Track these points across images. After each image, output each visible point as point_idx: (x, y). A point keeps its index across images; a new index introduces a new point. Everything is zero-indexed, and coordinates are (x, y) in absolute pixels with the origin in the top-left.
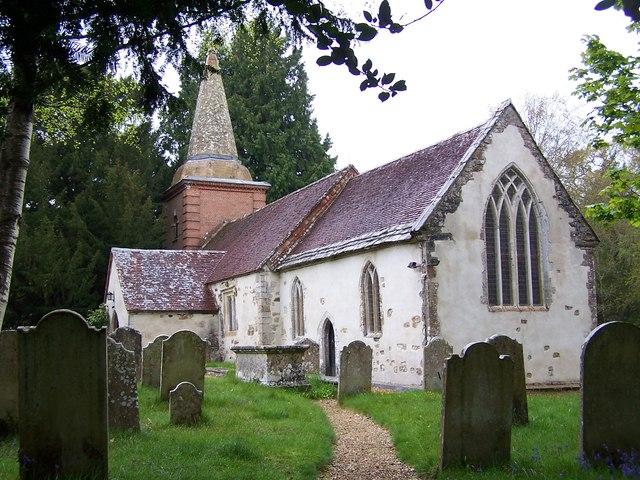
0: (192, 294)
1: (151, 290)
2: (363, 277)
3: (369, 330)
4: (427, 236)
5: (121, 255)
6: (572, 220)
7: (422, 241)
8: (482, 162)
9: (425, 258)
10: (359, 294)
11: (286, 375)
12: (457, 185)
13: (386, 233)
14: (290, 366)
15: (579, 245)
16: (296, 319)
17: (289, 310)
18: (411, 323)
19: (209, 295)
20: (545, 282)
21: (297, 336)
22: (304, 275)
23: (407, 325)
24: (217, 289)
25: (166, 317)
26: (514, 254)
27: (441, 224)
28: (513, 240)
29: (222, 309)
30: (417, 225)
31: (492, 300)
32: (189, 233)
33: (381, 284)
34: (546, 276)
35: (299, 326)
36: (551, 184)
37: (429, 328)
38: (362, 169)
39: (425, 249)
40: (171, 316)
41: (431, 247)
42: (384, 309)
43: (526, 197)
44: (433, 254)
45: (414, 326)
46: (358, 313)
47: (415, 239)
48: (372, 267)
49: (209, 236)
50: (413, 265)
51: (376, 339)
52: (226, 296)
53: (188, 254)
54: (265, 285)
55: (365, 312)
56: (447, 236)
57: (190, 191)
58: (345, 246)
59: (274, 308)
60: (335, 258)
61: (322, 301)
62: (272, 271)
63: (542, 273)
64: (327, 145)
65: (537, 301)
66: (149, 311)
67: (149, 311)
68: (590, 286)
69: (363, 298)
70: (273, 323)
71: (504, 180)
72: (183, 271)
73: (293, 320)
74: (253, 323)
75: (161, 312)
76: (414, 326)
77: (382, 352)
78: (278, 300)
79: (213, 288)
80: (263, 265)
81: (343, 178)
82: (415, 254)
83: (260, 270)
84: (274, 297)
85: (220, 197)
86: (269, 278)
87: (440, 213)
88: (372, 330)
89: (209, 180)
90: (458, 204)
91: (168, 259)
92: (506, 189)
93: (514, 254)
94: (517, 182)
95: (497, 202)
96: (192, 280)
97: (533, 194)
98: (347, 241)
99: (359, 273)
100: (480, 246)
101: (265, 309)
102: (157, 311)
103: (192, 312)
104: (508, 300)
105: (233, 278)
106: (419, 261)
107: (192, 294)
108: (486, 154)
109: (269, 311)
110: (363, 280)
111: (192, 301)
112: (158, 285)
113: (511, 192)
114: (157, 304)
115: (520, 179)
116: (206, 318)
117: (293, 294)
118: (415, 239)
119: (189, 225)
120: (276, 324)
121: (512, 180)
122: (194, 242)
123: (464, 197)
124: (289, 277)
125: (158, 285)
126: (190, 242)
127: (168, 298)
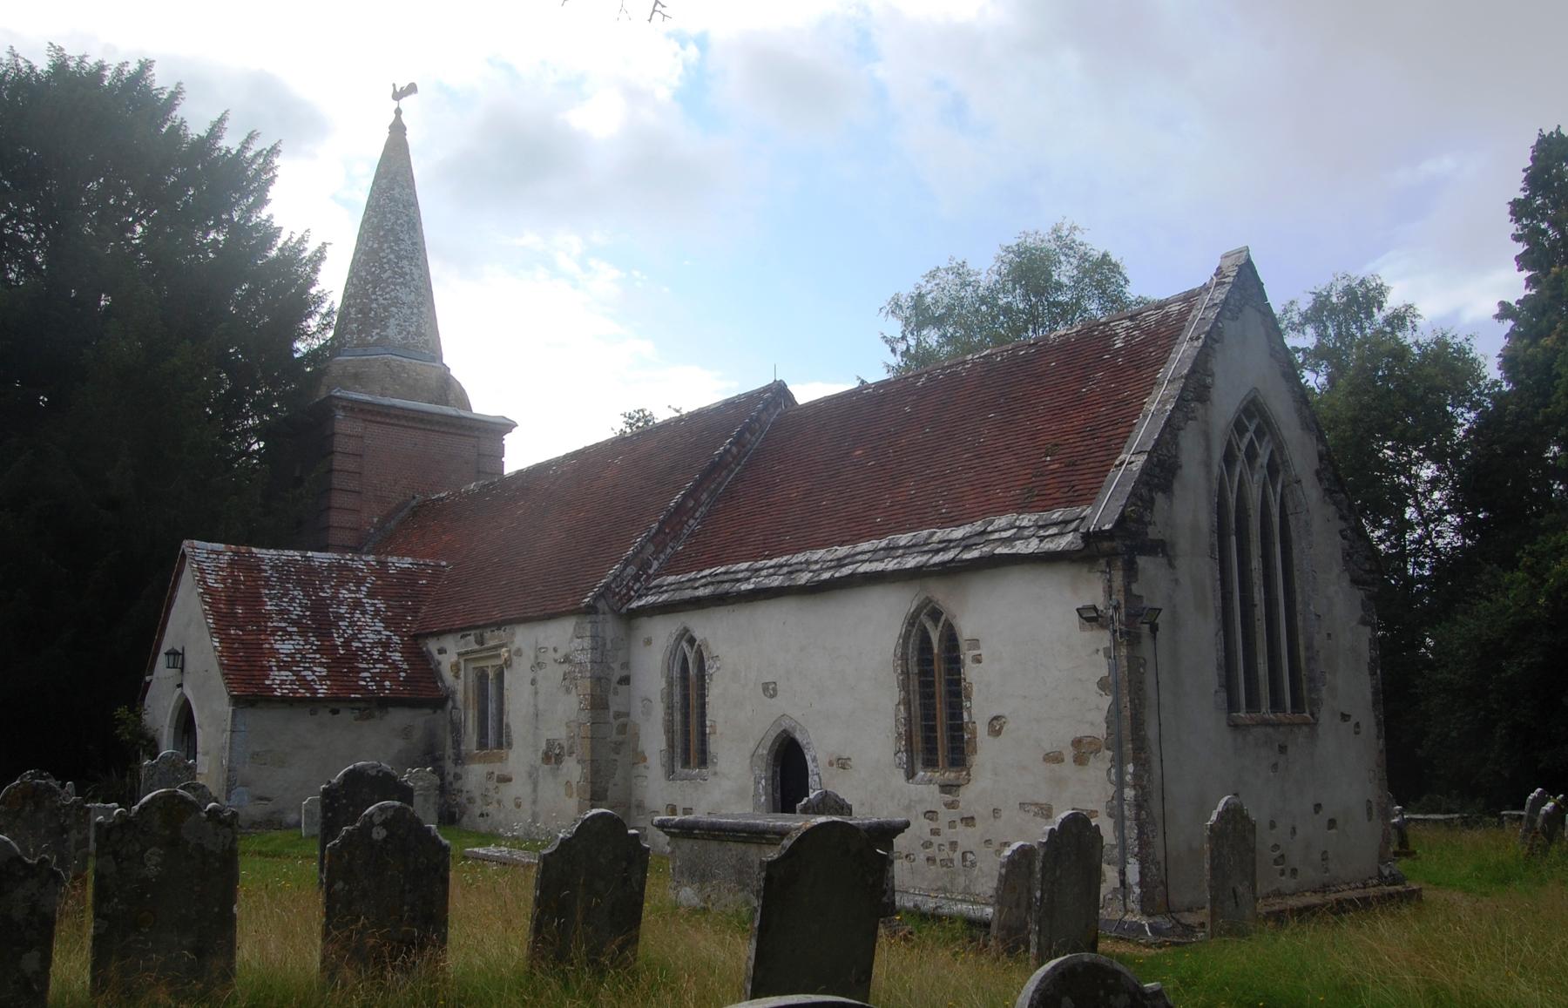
0: (384, 659)
2: (906, 638)
3: (919, 765)
4: (1118, 549)
5: (205, 559)
6: (1343, 525)
7: (1111, 556)
8: (1209, 380)
9: (1119, 597)
12: (1171, 429)
15: (1355, 582)
16: (678, 727)
17: (659, 711)
19: (423, 668)
20: (1308, 659)
21: (678, 768)
22: (712, 629)
23: (1054, 758)
24: (448, 654)
25: (324, 715)
26: (1258, 595)
27: (1147, 519)
28: (1256, 564)
29: (460, 696)
30: (1102, 513)
31: (1232, 706)
32: (335, 518)
33: (967, 655)
34: (1309, 647)
35: (691, 746)
37: (1130, 768)
38: (804, 394)
39: (1118, 579)
40: (335, 712)
41: (1131, 571)
42: (978, 710)
43: (1273, 469)
44: (1135, 588)
45: (1080, 760)
46: (891, 722)
47: (1092, 551)
48: (935, 615)
51: (947, 788)
52: (472, 665)
53: (367, 563)
54: (598, 645)
55: (909, 720)
56: (1160, 548)
59: (615, 704)
61: (770, 690)
62: (616, 613)
63: (1301, 640)
65: (1297, 705)
67: (284, 700)
68: (1373, 673)
69: (904, 686)
70: (614, 737)
71: (1240, 428)
73: (669, 731)
74: (560, 734)
76: (1080, 760)
77: (969, 821)
78: (625, 680)
79: (432, 646)
80: (596, 598)
81: (765, 409)
82: (1092, 590)
83: (591, 610)
84: (618, 673)
86: (610, 628)
87: (1144, 491)
88: (930, 763)
89: (386, 401)
90: (1174, 475)
92: (1243, 448)
93: (1258, 595)
94: (1259, 433)
95: (1230, 475)
96: (380, 626)
97: (1284, 462)
98: (842, 551)
101: (598, 704)
102: (302, 700)
104: (1252, 704)
105: (499, 625)
107: (384, 659)
108: (1217, 365)
109: (606, 707)
111: (384, 675)
113: (1251, 455)
115: (1267, 427)
116: (417, 719)
118: (1092, 551)
119: (338, 500)
120: (620, 738)
121: (1252, 428)
123: (1184, 458)
124: (661, 634)
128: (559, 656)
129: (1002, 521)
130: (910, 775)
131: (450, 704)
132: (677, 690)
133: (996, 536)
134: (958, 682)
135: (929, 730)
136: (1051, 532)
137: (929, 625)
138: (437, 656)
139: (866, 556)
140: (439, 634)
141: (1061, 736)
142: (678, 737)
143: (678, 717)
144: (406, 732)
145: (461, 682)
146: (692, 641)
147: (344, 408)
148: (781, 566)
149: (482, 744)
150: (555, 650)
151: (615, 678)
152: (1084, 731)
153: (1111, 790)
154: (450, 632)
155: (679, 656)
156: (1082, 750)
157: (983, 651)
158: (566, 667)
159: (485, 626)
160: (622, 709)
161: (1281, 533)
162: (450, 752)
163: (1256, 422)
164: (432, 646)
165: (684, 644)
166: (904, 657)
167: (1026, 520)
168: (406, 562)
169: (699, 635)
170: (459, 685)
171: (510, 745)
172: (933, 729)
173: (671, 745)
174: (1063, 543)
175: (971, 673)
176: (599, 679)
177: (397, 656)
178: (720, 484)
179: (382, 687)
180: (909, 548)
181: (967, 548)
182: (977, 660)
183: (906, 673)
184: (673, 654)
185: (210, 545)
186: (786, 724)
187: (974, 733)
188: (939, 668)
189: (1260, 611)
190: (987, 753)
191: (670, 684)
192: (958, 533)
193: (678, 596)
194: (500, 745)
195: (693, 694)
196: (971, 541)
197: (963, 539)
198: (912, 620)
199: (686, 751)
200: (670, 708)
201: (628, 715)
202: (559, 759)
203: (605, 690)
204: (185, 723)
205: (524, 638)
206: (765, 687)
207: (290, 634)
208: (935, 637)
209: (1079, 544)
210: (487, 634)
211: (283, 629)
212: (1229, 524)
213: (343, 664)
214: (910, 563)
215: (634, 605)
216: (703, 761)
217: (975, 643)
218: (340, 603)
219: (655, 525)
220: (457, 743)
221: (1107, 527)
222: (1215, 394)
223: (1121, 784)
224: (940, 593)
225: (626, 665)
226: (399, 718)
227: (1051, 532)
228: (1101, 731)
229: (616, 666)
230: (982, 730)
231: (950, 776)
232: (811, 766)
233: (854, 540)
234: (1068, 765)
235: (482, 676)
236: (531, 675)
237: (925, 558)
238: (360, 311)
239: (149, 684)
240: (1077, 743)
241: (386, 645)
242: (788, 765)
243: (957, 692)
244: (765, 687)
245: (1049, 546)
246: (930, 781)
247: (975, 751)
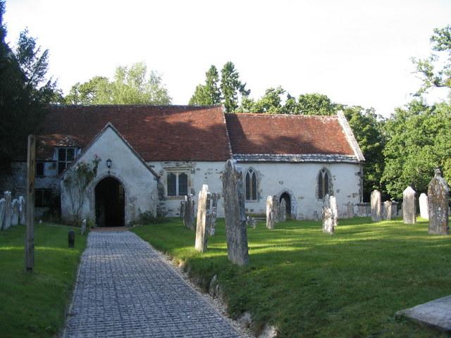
18: (352, 196)
23: (349, 196)
46: (315, 190)
76: (354, 197)
141: (351, 193)
146: (251, 171)
152: (355, 192)
154: (158, 161)
156: (354, 195)
186: (286, 190)
188: (323, 180)
193: (251, 160)
205: (203, 166)
206: (280, 182)
210: (181, 163)
214: (325, 161)
224: (327, 167)
228: (358, 192)
234: (352, 198)
236: (205, 176)
240: (354, 194)
244: (280, 182)
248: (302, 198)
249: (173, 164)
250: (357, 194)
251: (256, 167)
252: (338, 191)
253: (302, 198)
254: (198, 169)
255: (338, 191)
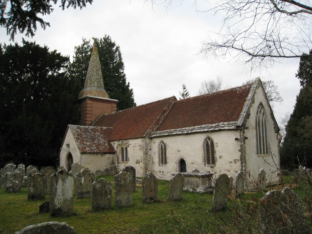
0: (104, 145)
1: (88, 144)
10: (202, 149)
11: (207, 186)
13: (218, 125)
14: (208, 182)
16: (161, 157)
18: (233, 162)
19: (111, 148)
20: (269, 145)
21: (161, 165)
22: (166, 140)
23: (231, 162)
25: (95, 155)
26: (262, 135)
28: (261, 130)
29: (118, 152)
31: (258, 154)
33: (215, 145)
34: (269, 143)
35: (164, 160)
36: (269, 109)
42: (217, 155)
44: (244, 135)
48: (209, 139)
49: (95, 120)
50: (236, 139)
51: (212, 167)
53: (99, 128)
54: (146, 144)
55: (205, 156)
57: (88, 102)
58: (194, 129)
59: (149, 153)
60: (188, 134)
63: (268, 142)
64: (128, 86)
65: (267, 153)
66: (90, 153)
69: (204, 151)
70: (149, 159)
72: (99, 136)
73: (159, 158)
74: (139, 159)
75: (94, 153)
76: (235, 163)
78: (150, 149)
79: (112, 143)
82: (237, 135)
83: (144, 137)
85: (100, 104)
86: (148, 140)
90: (249, 116)
91: (92, 129)
93: (262, 135)
98: (192, 128)
99: (203, 141)
100: (254, 132)
101: (146, 153)
102: (92, 153)
103: (105, 153)
104: (261, 153)
106: (239, 138)
108: (255, 97)
110: (204, 144)
111: (105, 148)
112: (90, 141)
114: (91, 149)
117: (159, 147)
118: (238, 128)
121: (260, 107)
122: (88, 122)
123: (251, 113)
124: (157, 141)
125: (90, 141)
126: (88, 122)
127: (96, 147)
128: (139, 145)
129: (222, 123)
130: (205, 165)
131: (116, 153)
132: (160, 151)
133: (220, 126)
134: (213, 150)
135: (208, 158)
136: (230, 125)
137: (208, 141)
138: (113, 145)
139: (197, 128)
140: (113, 141)
142: (161, 159)
143: (161, 156)
144: (109, 158)
145: (118, 149)
146: (163, 143)
147: (89, 99)
148: (180, 130)
149: (123, 160)
150: (138, 144)
151: (149, 149)
153: (241, 167)
154: (116, 141)
155: (161, 145)
157: (218, 145)
158: (140, 147)
159: (123, 140)
160: (150, 154)
161: (265, 125)
162: (116, 162)
163: (261, 106)
164: (112, 143)
165: (162, 143)
166: (204, 146)
167: (225, 123)
168: (105, 128)
169: (165, 141)
170: (118, 151)
171: (129, 161)
172: (209, 158)
173: (159, 161)
174: (232, 128)
175: (216, 149)
176: (146, 149)
177: (106, 145)
178: (165, 115)
179: (104, 150)
180: (205, 127)
181: (216, 128)
182: (217, 146)
183: (204, 149)
184: (159, 145)
185: (73, 125)
186: (182, 157)
187: (217, 158)
188: (210, 148)
189: (262, 138)
190: (219, 162)
191: (159, 150)
192: (214, 125)
193: (160, 135)
194: (127, 160)
195: (163, 152)
196: (216, 127)
197: (215, 126)
198: (205, 140)
199: (162, 161)
200: (159, 154)
201: (151, 155)
202: (139, 163)
203: (147, 151)
204: (70, 157)
205: (132, 142)
207: (88, 141)
208: (209, 142)
209: (235, 128)
210: (124, 141)
211: (87, 140)
212: (258, 123)
213: (98, 146)
214: (206, 130)
215: (152, 136)
216: (166, 163)
217: (217, 144)
218: (96, 136)
219: (155, 122)
220: (118, 160)
221: (240, 125)
222: (255, 102)
223: (242, 167)
225: (150, 147)
226: (108, 156)
227: (230, 125)
228: (239, 159)
229: (149, 147)
230: (218, 158)
231: (212, 165)
232: (187, 164)
233: (194, 126)
234: (233, 164)
235: (122, 149)
237: (208, 129)
238: (90, 80)
239: (61, 150)
240: (235, 160)
241: (104, 143)
242: (182, 163)
243: (213, 152)
245: (230, 128)
246: (209, 166)
247: (217, 161)
248: (192, 163)
249: (121, 142)
250: (238, 160)
251: (165, 140)
252: (221, 157)
253: (192, 163)
254: (130, 144)
255: (221, 157)
